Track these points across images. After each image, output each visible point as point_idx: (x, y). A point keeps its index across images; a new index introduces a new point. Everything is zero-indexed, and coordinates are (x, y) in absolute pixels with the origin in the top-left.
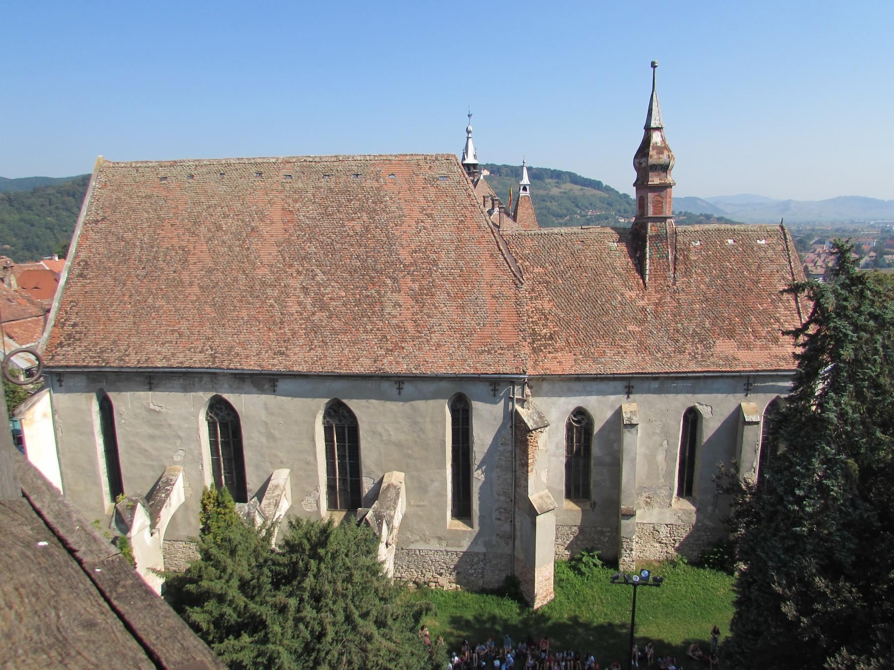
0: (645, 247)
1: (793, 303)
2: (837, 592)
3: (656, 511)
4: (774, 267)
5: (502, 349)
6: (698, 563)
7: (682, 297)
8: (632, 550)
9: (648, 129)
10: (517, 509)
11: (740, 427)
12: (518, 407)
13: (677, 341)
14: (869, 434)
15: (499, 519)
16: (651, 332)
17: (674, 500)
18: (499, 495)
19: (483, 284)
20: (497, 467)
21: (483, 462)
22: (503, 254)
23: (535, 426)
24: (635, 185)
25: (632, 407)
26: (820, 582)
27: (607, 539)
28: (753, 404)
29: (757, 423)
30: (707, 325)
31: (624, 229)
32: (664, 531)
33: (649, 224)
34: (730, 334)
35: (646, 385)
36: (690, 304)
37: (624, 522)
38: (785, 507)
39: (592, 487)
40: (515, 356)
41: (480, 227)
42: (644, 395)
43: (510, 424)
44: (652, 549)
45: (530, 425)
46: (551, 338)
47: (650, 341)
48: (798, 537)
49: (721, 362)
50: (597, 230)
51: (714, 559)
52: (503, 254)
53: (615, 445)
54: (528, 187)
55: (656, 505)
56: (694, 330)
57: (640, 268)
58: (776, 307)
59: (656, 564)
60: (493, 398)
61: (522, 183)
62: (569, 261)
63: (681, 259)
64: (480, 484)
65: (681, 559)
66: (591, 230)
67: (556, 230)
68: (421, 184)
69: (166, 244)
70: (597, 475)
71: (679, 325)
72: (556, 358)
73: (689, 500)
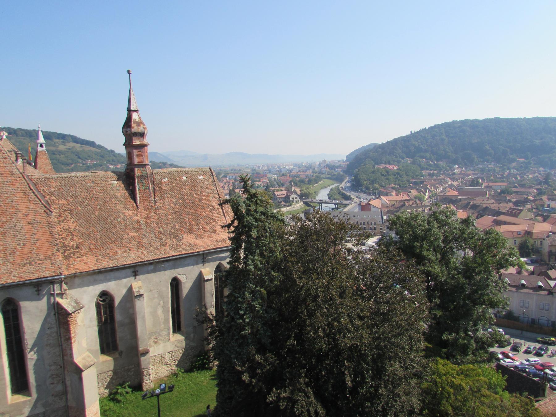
0: (135, 183)
1: (221, 210)
2: (266, 360)
3: (161, 345)
4: (209, 191)
5: (41, 260)
6: (189, 370)
7: (161, 212)
8: (150, 375)
9: (129, 111)
10: (66, 372)
12: (58, 299)
13: (161, 239)
14: (269, 274)
15: (53, 384)
16: (145, 235)
17: (171, 336)
18: (50, 366)
19: (20, 215)
20: (47, 345)
21: (34, 346)
22: (34, 193)
23: (73, 310)
24: (124, 145)
25: (138, 284)
26: (258, 357)
27: (132, 373)
28: (208, 269)
29: (211, 279)
30: (177, 227)
31: (120, 172)
32: (168, 357)
33: (136, 169)
34: (191, 231)
35: (145, 269)
36: (166, 216)
37: (142, 359)
38: (236, 322)
39: (118, 342)
40: (52, 264)
41: (12, 173)
42: (145, 275)
43: (53, 313)
44: (162, 370)
45: (70, 310)
46: (77, 247)
47: (145, 241)
48: (244, 337)
49: (188, 248)
50: (103, 173)
51: (199, 364)
52: (34, 193)
53: (131, 311)
54: (44, 145)
55: (161, 342)
56: (170, 231)
57: (133, 197)
58: (212, 213)
59: (166, 379)
60: (38, 296)
61: (39, 142)
63: (157, 189)
64: (33, 362)
65: (180, 371)
66: (98, 174)
67: (73, 174)
70: (120, 333)
71: (161, 229)
72: (82, 261)
73: (180, 334)
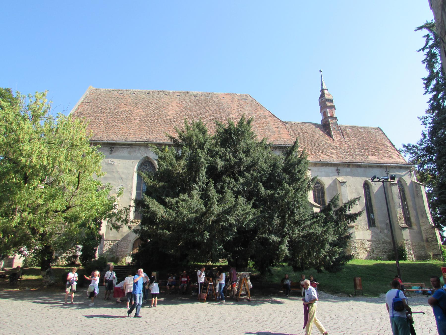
9: (322, 90)
11: (389, 188)
55: (360, 229)
62: (300, 131)
68: (236, 100)
69: (122, 109)
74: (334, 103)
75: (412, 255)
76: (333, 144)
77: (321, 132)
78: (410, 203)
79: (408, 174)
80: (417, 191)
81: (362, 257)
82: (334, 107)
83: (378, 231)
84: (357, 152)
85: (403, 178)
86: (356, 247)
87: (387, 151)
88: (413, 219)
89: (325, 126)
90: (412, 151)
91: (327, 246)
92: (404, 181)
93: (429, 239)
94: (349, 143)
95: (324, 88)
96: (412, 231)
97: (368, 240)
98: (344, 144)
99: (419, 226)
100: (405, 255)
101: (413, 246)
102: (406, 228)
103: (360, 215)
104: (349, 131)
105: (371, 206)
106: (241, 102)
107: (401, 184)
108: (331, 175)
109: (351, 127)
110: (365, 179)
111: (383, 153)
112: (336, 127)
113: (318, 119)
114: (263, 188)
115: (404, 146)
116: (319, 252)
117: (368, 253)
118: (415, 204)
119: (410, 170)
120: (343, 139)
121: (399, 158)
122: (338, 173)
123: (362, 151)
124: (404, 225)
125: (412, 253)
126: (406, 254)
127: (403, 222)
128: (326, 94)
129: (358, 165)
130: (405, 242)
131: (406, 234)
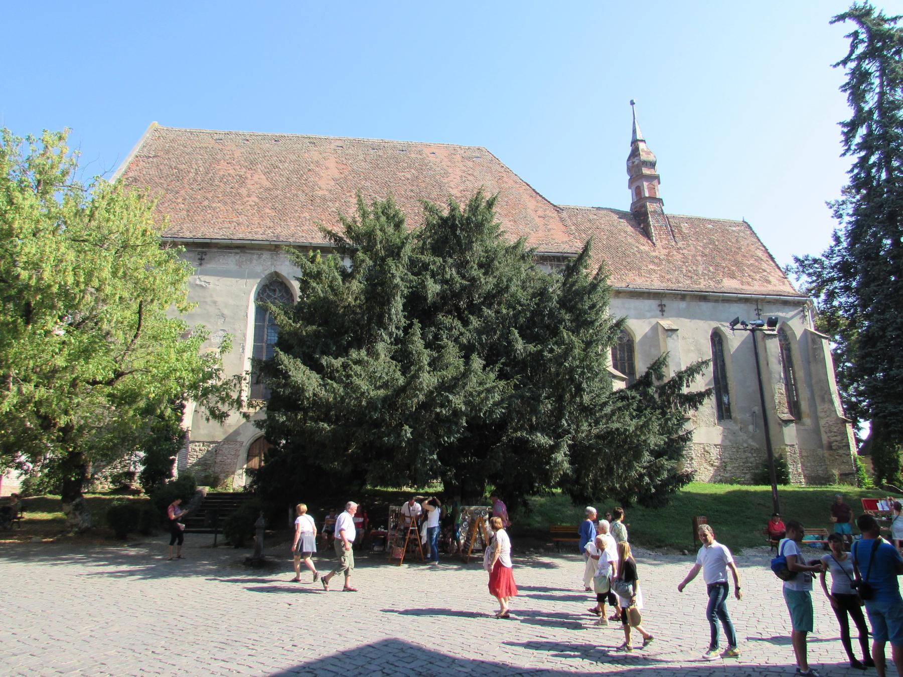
9: (635, 142)
55: (702, 424)
62: (588, 225)
68: (458, 158)
69: (222, 173)
74: (659, 170)
75: (799, 474)
76: (654, 254)
77: (630, 229)
78: (800, 374)
79: (799, 316)
80: (814, 349)
81: (703, 477)
82: (657, 178)
83: (736, 428)
84: (700, 269)
85: (789, 323)
86: (692, 459)
87: (758, 270)
88: (804, 406)
89: (639, 217)
90: (811, 271)
91: (647, 457)
92: (791, 329)
93: (835, 443)
94: (684, 251)
95: (638, 138)
96: (802, 427)
97: (716, 445)
98: (675, 253)
99: (816, 418)
100: (787, 474)
101: (801, 457)
102: (791, 421)
103: (708, 396)
104: (685, 227)
105: (724, 377)
106: (470, 164)
107: (785, 337)
108: (649, 314)
109: (689, 219)
110: (715, 324)
111: (751, 273)
112: (660, 218)
113: (625, 201)
114: (520, 339)
115: (797, 260)
116: (629, 467)
117: (716, 471)
118: (809, 375)
119: (804, 308)
120: (673, 244)
121: (784, 283)
122: (662, 311)
123: (711, 268)
124: (787, 416)
125: (800, 471)
126: (789, 473)
127: (786, 410)
128: (643, 151)
129: (702, 297)
130: (788, 449)
131: (790, 435)
